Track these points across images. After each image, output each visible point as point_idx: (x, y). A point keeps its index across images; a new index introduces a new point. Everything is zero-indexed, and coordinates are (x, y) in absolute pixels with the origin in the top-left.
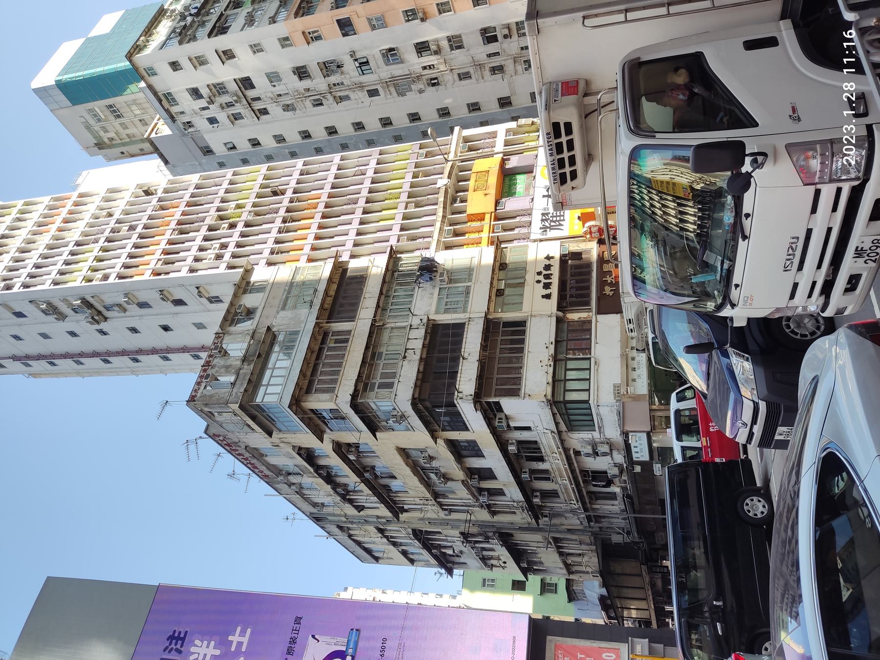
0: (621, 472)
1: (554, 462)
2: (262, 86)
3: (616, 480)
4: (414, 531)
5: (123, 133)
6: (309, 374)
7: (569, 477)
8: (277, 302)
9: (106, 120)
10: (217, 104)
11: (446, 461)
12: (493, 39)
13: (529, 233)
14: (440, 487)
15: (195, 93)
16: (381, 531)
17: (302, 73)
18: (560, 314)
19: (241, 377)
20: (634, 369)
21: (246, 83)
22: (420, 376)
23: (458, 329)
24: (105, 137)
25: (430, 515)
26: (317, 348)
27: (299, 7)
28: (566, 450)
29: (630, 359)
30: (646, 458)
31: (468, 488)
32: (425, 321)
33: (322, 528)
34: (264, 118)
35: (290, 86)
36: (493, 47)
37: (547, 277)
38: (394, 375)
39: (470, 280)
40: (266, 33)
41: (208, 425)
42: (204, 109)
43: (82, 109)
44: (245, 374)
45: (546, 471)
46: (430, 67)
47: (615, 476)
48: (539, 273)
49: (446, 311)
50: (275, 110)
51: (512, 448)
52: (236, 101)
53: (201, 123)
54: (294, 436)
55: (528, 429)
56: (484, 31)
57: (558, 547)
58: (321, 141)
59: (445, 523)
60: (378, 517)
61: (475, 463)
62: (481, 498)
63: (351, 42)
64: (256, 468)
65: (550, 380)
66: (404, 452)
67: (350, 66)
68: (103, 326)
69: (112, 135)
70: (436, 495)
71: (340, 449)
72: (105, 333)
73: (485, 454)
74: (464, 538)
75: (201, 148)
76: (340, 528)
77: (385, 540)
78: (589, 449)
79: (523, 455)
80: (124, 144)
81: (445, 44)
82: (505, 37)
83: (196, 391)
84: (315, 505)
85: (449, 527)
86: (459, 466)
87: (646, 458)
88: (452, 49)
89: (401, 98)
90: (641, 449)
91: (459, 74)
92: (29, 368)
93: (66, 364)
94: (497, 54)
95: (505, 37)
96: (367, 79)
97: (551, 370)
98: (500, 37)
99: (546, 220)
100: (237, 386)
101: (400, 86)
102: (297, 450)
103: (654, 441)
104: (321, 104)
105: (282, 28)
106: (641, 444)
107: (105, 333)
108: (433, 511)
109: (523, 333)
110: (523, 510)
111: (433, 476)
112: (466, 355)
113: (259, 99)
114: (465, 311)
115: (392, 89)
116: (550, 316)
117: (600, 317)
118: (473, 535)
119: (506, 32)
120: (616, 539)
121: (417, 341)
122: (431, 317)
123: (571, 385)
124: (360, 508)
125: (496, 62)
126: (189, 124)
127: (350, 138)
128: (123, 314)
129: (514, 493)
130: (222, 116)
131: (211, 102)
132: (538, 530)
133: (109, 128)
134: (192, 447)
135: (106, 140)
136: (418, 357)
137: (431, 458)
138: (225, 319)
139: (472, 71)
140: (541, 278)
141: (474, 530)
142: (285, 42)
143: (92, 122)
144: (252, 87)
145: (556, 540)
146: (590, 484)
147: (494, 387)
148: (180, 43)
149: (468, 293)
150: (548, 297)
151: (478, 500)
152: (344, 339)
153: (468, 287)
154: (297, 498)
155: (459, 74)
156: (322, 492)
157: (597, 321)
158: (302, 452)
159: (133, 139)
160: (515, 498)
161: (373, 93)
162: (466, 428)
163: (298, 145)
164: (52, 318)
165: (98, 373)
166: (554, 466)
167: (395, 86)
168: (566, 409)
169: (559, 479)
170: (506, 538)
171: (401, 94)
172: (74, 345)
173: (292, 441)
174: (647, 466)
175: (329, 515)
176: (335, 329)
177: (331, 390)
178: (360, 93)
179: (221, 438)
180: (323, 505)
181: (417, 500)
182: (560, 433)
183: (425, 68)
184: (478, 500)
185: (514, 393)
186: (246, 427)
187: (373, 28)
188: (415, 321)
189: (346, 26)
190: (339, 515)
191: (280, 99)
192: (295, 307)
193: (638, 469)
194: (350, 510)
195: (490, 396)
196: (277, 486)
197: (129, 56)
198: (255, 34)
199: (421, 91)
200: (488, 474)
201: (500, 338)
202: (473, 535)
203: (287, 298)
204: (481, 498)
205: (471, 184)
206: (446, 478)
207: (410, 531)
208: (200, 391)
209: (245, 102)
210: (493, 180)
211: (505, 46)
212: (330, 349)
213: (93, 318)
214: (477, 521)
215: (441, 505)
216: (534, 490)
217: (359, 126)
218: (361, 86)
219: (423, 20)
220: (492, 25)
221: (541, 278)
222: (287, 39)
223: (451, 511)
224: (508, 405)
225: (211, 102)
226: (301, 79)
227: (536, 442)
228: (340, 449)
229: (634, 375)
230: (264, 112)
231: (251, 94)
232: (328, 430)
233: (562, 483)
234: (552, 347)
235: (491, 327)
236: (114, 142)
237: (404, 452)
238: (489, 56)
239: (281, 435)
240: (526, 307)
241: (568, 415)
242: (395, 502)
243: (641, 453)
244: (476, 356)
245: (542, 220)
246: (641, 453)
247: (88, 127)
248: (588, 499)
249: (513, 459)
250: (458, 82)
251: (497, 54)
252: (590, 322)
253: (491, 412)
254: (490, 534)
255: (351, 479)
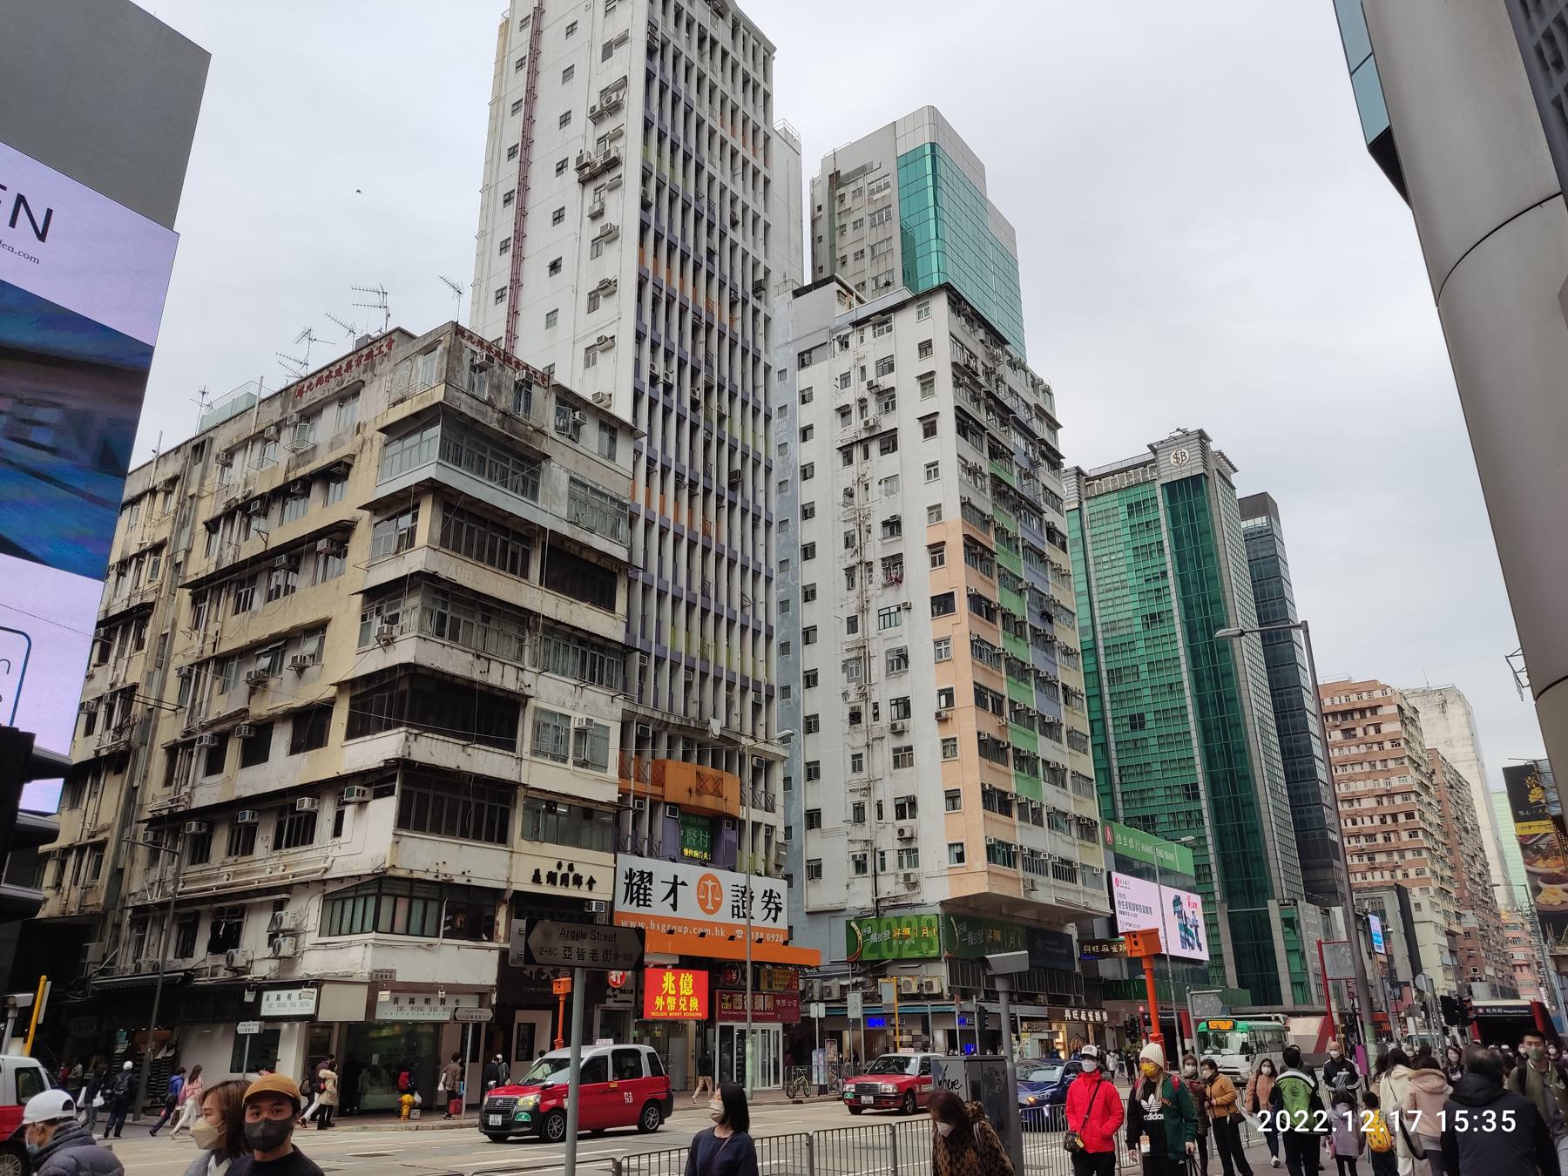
0: (235, 970)
1: (268, 863)
2: (880, 464)
3: (221, 960)
4: (151, 606)
5: (849, 221)
6: (474, 510)
7: (232, 885)
8: (583, 473)
9: (870, 201)
10: (867, 395)
11: (288, 693)
12: (901, 815)
13: (625, 852)
14: (241, 675)
15: (887, 366)
16: (157, 549)
17: (893, 526)
18: (508, 896)
19: (482, 407)
20: (412, 1001)
21: (889, 442)
22: (448, 679)
23: (504, 739)
24: (848, 190)
25: (180, 642)
26: (510, 526)
27: (977, 543)
28: (288, 888)
29: (413, 995)
30: (266, 1011)
31: (229, 717)
32: (527, 692)
33: (178, 449)
34: (840, 458)
35: (876, 506)
36: (890, 811)
37: (565, 879)
38: (454, 637)
39: (575, 763)
40: (949, 490)
41: (412, 337)
42: (863, 369)
43: (890, 167)
44: (485, 415)
45: (248, 850)
46: (876, 715)
47: (230, 959)
48: (571, 867)
49: (537, 727)
50: (849, 476)
51: (306, 804)
52: (867, 423)
53: (843, 362)
54: (374, 463)
55: (337, 832)
56: (913, 803)
57: (81, 849)
58: (796, 532)
59: (161, 664)
60: (188, 552)
61: (281, 739)
62: (208, 734)
63: (923, 607)
64: (320, 382)
65: (416, 875)
66: (319, 628)
67: (891, 598)
68: (571, 175)
69: (848, 202)
70: (223, 662)
71: (339, 535)
72: (559, 170)
73: (295, 757)
74: (123, 691)
75: (809, 351)
76: (172, 481)
77: (134, 550)
78: (288, 923)
79: (291, 817)
80: (831, 215)
81: (904, 742)
82: (901, 832)
83: (470, 338)
84: (230, 453)
85: (150, 666)
86: (279, 711)
87: (266, 1011)
88: (896, 750)
89: (840, 665)
90: (294, 1005)
91: (860, 755)
92: (517, 24)
93: (517, 86)
94: (880, 816)
95: (901, 832)
96: (871, 622)
97: (430, 877)
98: (901, 823)
99: (642, 879)
100: (469, 400)
101: (856, 664)
102: (347, 460)
103: (291, 1027)
104: (847, 546)
105: (952, 512)
106: (294, 1005)
107: (559, 170)
108: (187, 648)
109: (489, 839)
110: (172, 801)
111: (265, 662)
112: (469, 750)
113: (866, 456)
114: (535, 753)
115: (853, 655)
116: (508, 881)
117: (496, 954)
118: (126, 710)
119: (907, 835)
120: (94, 950)
121: (502, 677)
122: (532, 702)
123: (418, 907)
124: (212, 526)
125: (870, 813)
126: (844, 344)
127: (795, 578)
128: (587, 213)
129: (209, 792)
130: (849, 397)
131: (871, 386)
132: (127, 818)
133: (859, 202)
134: (376, 299)
135: (842, 191)
136: (477, 677)
137: (301, 671)
138: (568, 392)
139: (864, 775)
140: (565, 870)
141: (138, 709)
142: (935, 511)
143: (870, 177)
144: (884, 451)
145: (100, 847)
146: (225, 917)
147: (416, 790)
148: (955, 365)
149: (554, 758)
150: (536, 878)
151: (204, 729)
152: (518, 569)
153: (564, 760)
154: (249, 426)
155: (860, 755)
156: (258, 472)
157: (490, 949)
158: (343, 469)
159: (837, 233)
160: (198, 792)
161: (852, 625)
162: (351, 733)
163: (794, 496)
164: (595, 100)
165: (494, 132)
166: (258, 864)
167: (858, 659)
168: (366, 897)
169: (231, 869)
170: (116, 762)
171: (845, 666)
172: (546, 115)
173: (366, 454)
174: (252, 1012)
175: (205, 469)
176: (532, 555)
177: (444, 542)
178: (854, 605)
179: (385, 349)
180: (227, 464)
181: (217, 626)
182: (324, 882)
183: (876, 706)
184: (204, 729)
185: (403, 821)
186: (399, 396)
187: (937, 643)
188: (527, 677)
189: (943, 604)
190: (201, 484)
191: (862, 488)
192: (572, 497)
193: (249, 997)
194: (209, 508)
195: (403, 783)
196: (277, 403)
197: (947, 288)
198: (951, 471)
199: (845, 695)
200: (256, 752)
201: (486, 803)
202: (126, 710)
203: (585, 486)
204: (208, 734)
205: (708, 769)
206: (258, 685)
207: (150, 599)
208: (469, 344)
209: (864, 435)
210: (709, 802)
211: (889, 828)
212: (505, 543)
213: (587, 165)
214: (157, 718)
215: (202, 664)
216: (211, 829)
217: (809, 594)
218: (863, 610)
219: (938, 715)
220: (919, 814)
221: (565, 870)
222: (939, 518)
223: (185, 678)
224: (385, 809)
225: (871, 386)
226: (885, 524)
227: (311, 842)
228: (339, 535)
229: (404, 1002)
230: (848, 460)
231: (874, 448)
232: (377, 519)
233: (222, 871)
234: (463, 881)
235: (502, 792)
236: (837, 202)
237: (319, 628)
238: (879, 805)
239: (378, 445)
240: (526, 846)
241: (355, 899)
242: (220, 588)
243: (273, 1004)
244: (465, 767)
245: (642, 873)
246: (273, 1004)
247: (863, 170)
248: (185, 916)
249: (289, 801)
250: (850, 752)
251: (880, 816)
252: (490, 939)
253: (376, 781)
254: (125, 737)
255: (282, 528)
